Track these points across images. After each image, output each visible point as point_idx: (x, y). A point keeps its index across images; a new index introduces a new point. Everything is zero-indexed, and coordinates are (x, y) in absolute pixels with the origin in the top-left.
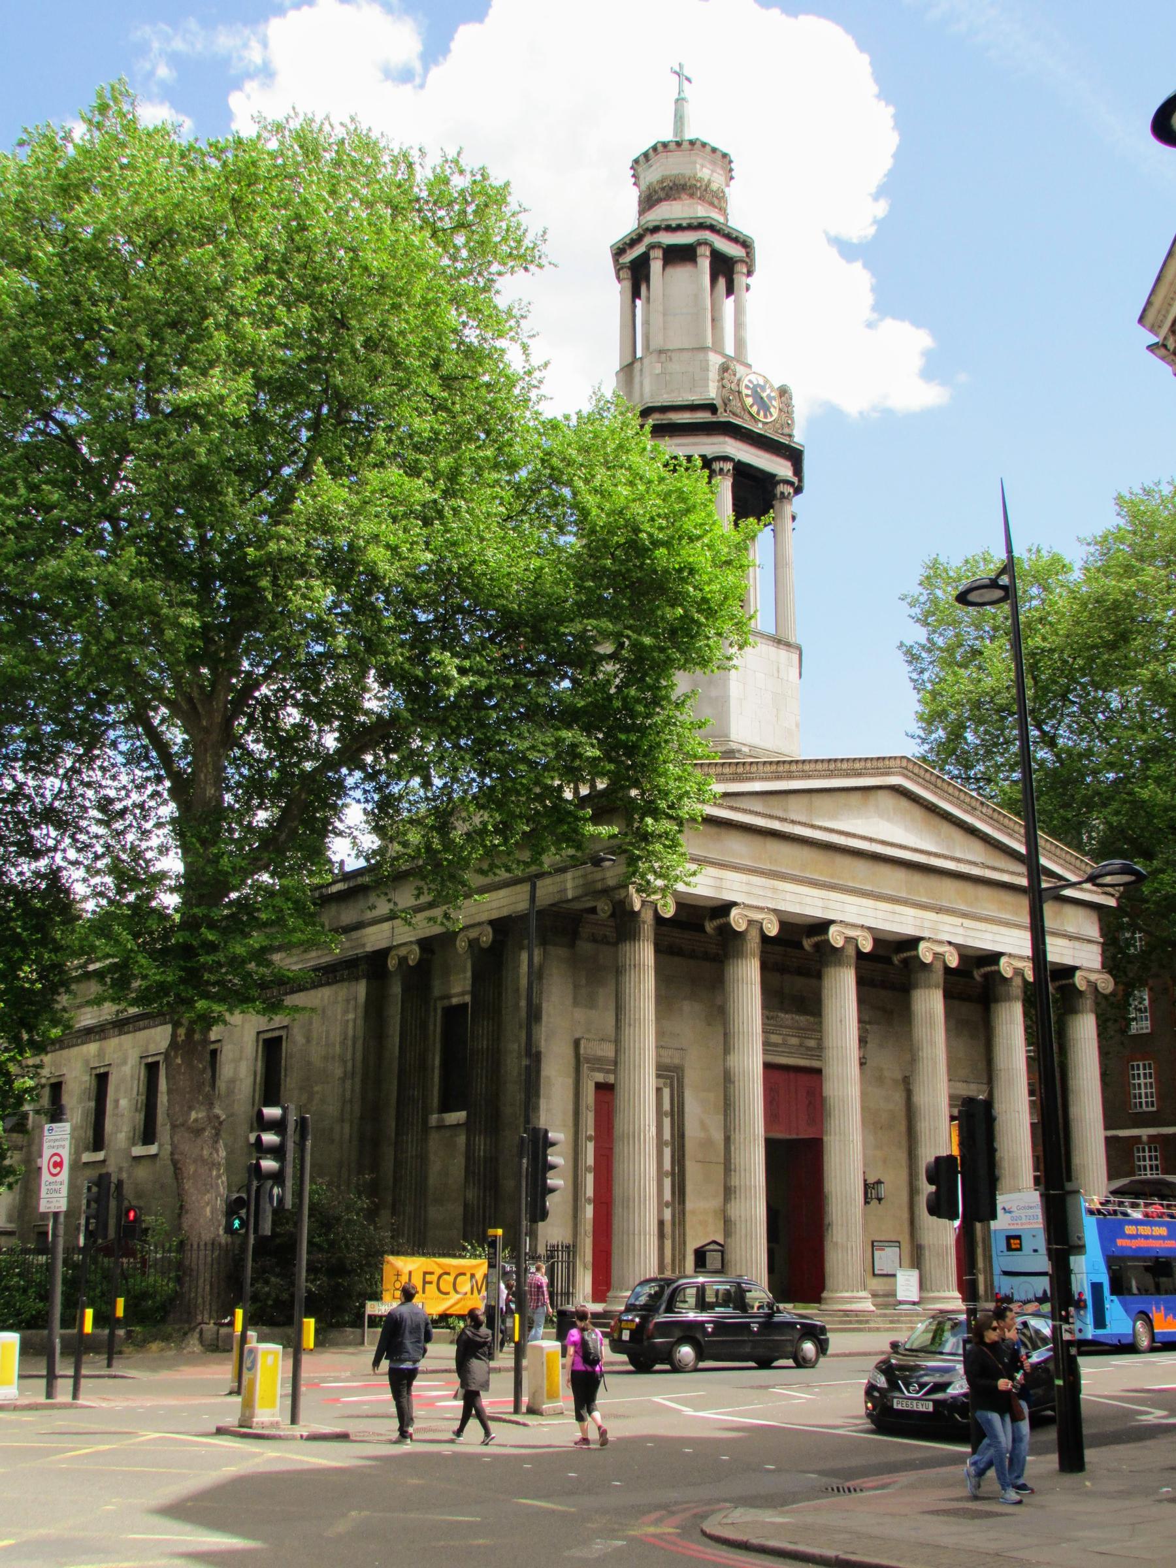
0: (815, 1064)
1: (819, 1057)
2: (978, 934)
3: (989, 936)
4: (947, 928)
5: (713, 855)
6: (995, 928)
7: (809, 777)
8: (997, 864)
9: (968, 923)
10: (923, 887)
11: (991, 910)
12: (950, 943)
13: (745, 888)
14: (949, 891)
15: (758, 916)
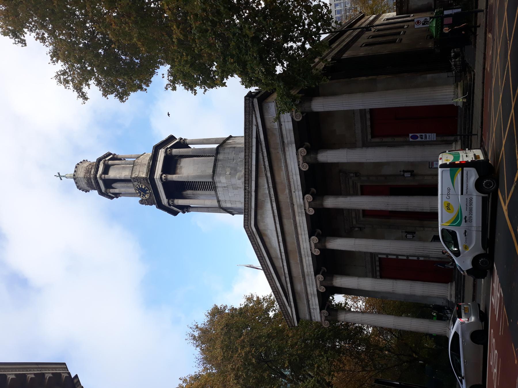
0: (361, 212)
1: (358, 210)
2: (295, 182)
3: (295, 178)
5: (304, 295)
6: (290, 174)
8: (263, 169)
9: (293, 190)
10: (286, 212)
11: (283, 173)
12: (303, 198)
14: (284, 198)
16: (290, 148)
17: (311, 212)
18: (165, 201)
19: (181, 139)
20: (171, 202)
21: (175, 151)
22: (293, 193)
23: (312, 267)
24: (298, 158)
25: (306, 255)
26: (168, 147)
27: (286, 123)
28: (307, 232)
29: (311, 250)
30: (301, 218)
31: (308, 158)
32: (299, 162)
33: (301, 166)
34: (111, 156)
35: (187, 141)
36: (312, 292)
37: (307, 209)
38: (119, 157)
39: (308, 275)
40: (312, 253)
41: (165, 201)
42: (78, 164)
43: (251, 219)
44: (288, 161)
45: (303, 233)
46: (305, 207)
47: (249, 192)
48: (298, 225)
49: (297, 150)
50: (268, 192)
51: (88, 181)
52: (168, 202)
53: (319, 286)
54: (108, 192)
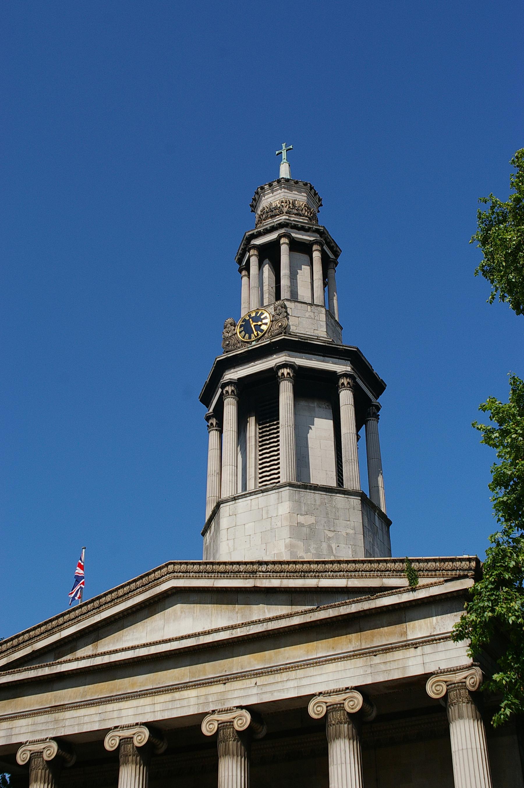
2: (279, 687)
3: (291, 684)
4: (236, 694)
6: (300, 673)
7: (79, 621)
9: (260, 680)
12: (241, 707)
13: (31, 729)
15: (39, 747)
16: (361, 671)
17: (208, 728)
18: (234, 374)
19: (378, 408)
20: (229, 389)
21: (346, 397)
22: (254, 681)
23: (76, 730)
24: (338, 692)
25: (103, 716)
26: (358, 380)
27: (419, 660)
28: (159, 717)
29: (116, 727)
30: (193, 701)
31: (339, 715)
32: (329, 694)
33: (320, 698)
34: (332, 256)
35: (372, 422)
36: (16, 731)
37: (215, 717)
38: (331, 272)
39: (56, 721)
40: (109, 730)
41: (234, 374)
42: (311, 188)
43: (190, 578)
44: (331, 667)
45: (158, 707)
46: (220, 712)
47: (254, 572)
48: (177, 695)
49: (357, 688)
50: (255, 618)
51: (276, 208)
52: (230, 383)
53: (31, 747)
54: (252, 252)
